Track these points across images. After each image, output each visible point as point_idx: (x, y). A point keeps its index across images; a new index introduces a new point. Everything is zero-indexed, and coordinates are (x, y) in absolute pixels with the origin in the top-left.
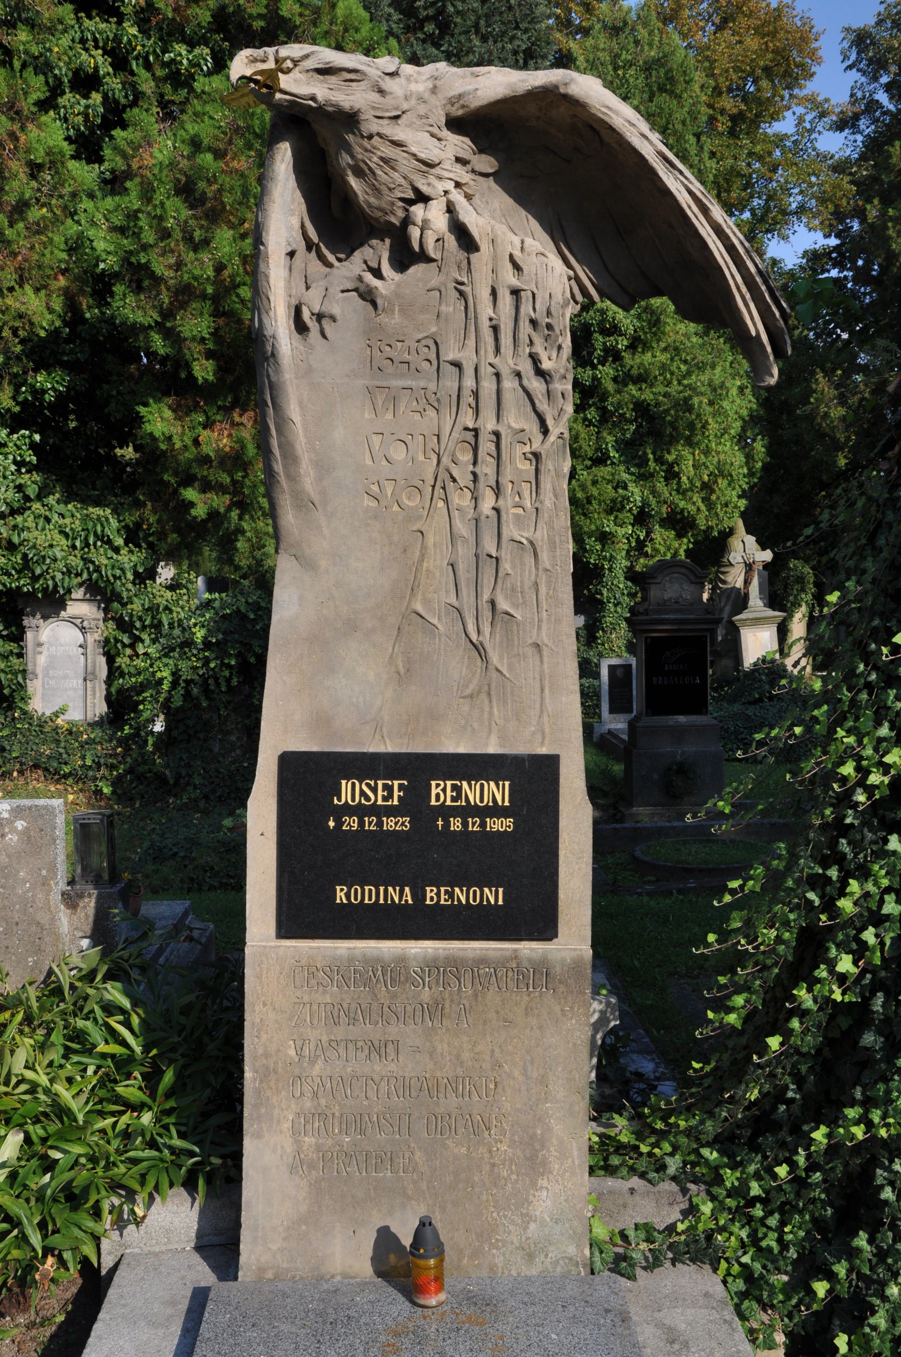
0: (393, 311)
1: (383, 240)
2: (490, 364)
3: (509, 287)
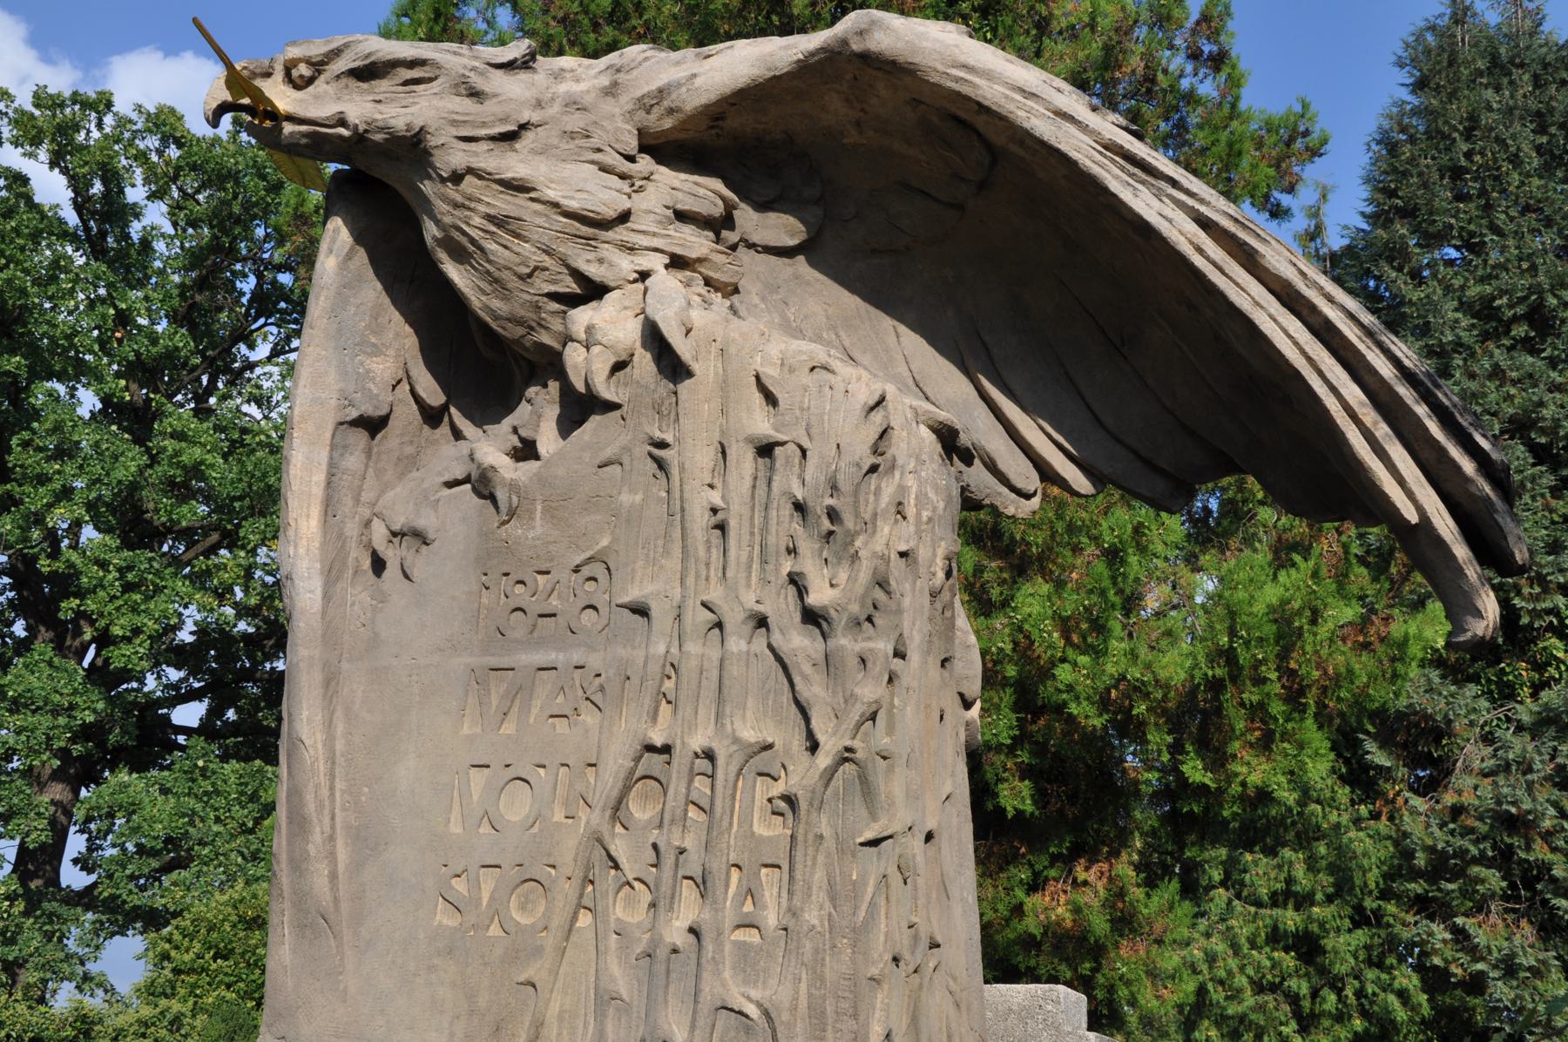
0: (532, 512)
1: (545, 386)
2: (704, 604)
3: (750, 440)
